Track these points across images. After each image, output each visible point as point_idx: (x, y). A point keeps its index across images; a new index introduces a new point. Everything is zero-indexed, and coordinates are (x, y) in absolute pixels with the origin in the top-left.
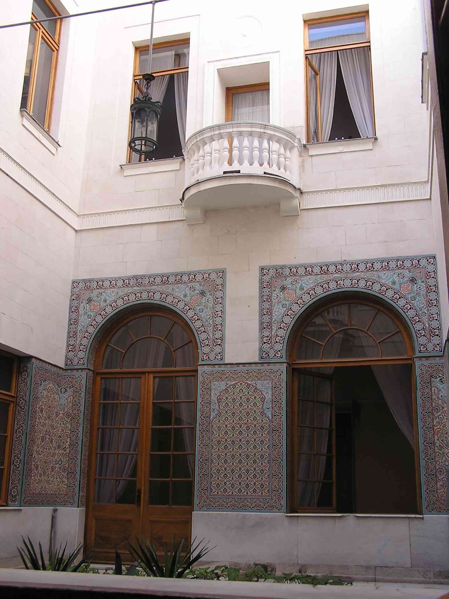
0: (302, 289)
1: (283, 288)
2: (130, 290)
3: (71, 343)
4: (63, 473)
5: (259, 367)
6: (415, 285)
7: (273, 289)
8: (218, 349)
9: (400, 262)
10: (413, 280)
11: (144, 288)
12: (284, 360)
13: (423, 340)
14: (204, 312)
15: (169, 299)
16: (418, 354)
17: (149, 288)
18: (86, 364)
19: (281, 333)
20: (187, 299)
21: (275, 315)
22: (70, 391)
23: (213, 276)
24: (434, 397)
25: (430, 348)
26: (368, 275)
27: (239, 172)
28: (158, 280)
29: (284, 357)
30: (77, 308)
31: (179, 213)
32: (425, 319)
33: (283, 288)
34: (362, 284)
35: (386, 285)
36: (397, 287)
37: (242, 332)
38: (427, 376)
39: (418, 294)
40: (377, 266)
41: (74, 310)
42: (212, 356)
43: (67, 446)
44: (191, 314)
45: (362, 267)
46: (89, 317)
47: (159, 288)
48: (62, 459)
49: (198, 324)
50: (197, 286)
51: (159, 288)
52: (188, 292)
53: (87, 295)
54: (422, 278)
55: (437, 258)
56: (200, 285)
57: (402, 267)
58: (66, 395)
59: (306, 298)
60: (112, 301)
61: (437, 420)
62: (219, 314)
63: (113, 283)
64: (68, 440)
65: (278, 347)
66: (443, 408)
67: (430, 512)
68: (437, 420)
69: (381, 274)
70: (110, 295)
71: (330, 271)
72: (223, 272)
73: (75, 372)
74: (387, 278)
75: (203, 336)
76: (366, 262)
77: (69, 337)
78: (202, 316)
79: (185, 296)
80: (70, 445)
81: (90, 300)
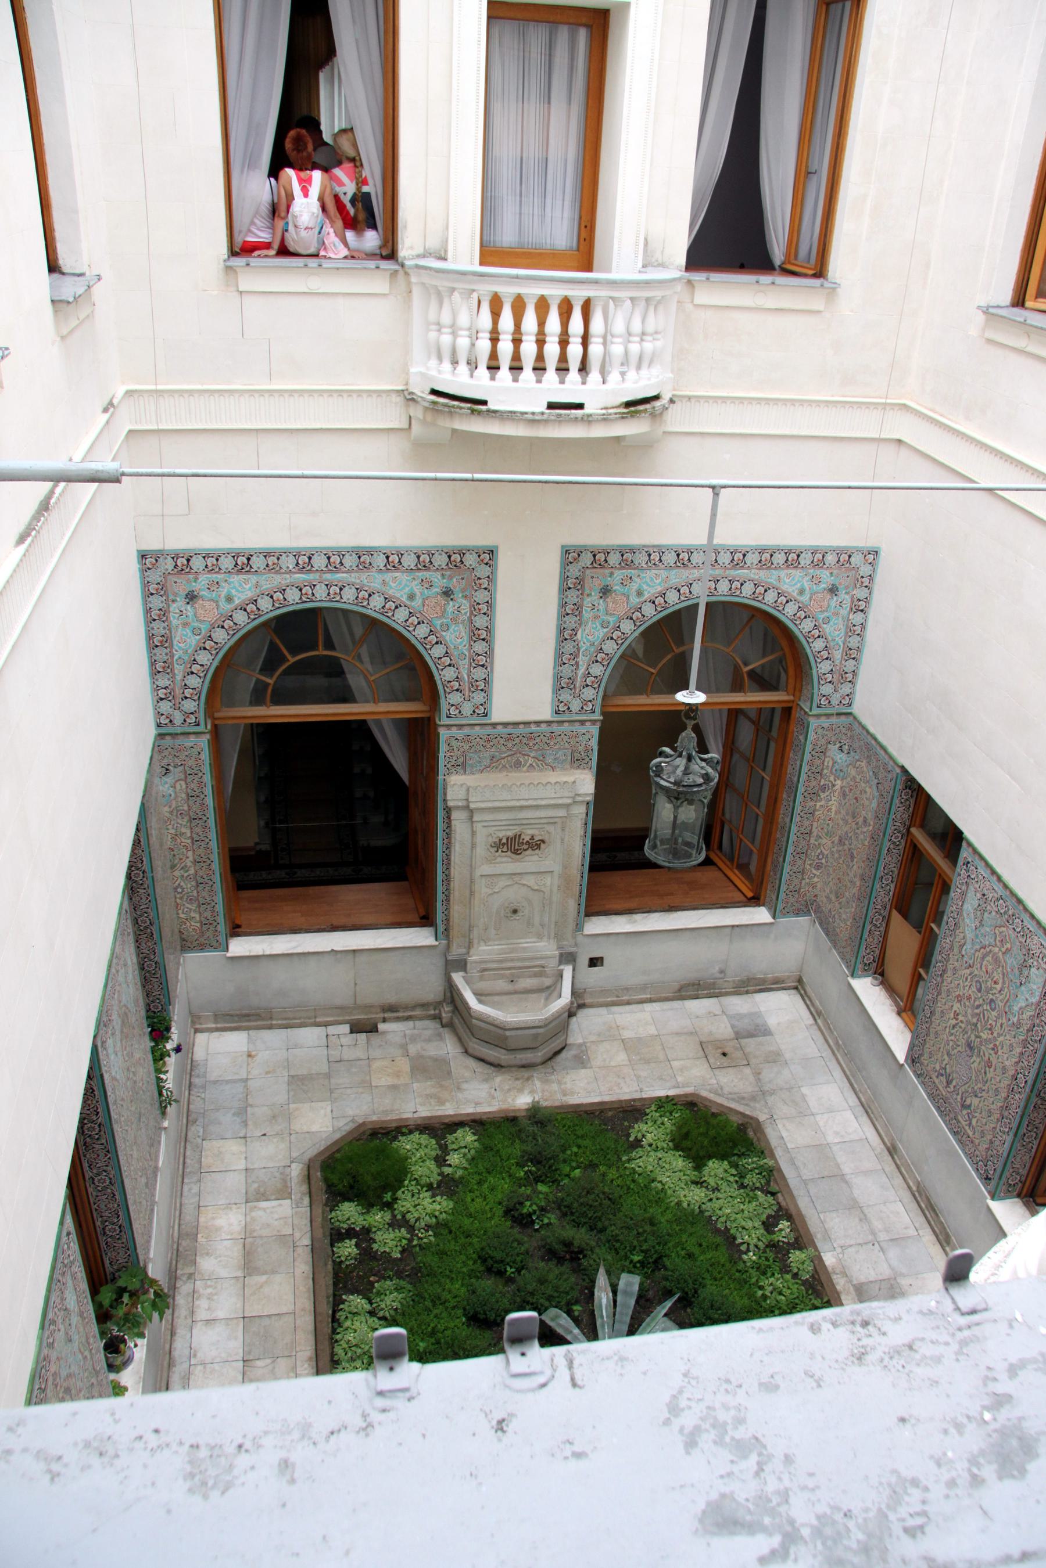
0: (639, 593)
1: (605, 591)
2: (288, 579)
3: (164, 681)
4: (189, 906)
5: (555, 728)
6: (835, 598)
7: (587, 591)
8: (479, 698)
9: (819, 557)
10: (833, 590)
11: (317, 576)
12: (597, 716)
13: (827, 689)
14: (451, 630)
15: (377, 602)
16: (815, 711)
17: (328, 576)
18: (202, 723)
19: (597, 670)
20: (417, 603)
21: (588, 641)
22: (176, 773)
23: (470, 560)
24: (825, 771)
25: (834, 702)
26: (762, 575)
27: (580, 406)
28: (350, 561)
29: (598, 710)
30: (164, 613)
31: (393, 417)
32: (837, 655)
33: (605, 591)
34: (748, 589)
35: (789, 594)
36: (805, 598)
37: (523, 669)
38: (823, 742)
39: (836, 614)
40: (779, 559)
41: (155, 619)
42: (467, 709)
43: (189, 864)
44: (422, 631)
45: (752, 559)
46: (196, 632)
47: (353, 578)
48: (182, 884)
49: (438, 651)
50: (436, 577)
51: (353, 578)
52: (417, 589)
53: (181, 586)
54: (847, 587)
55: (882, 554)
56: (443, 575)
57: (820, 564)
58: (169, 779)
59: (649, 610)
60: (245, 600)
61: (822, 803)
62: (483, 635)
63: (243, 562)
64: (190, 854)
65: (589, 693)
66: (834, 786)
67: (784, 915)
68: (822, 803)
69: (783, 573)
70: (242, 588)
71: (694, 561)
72: (492, 552)
73: (180, 741)
74: (791, 581)
75: (449, 674)
76: (762, 551)
77: (155, 673)
78: (447, 638)
79: (411, 597)
80: (195, 862)
81: (191, 597)
